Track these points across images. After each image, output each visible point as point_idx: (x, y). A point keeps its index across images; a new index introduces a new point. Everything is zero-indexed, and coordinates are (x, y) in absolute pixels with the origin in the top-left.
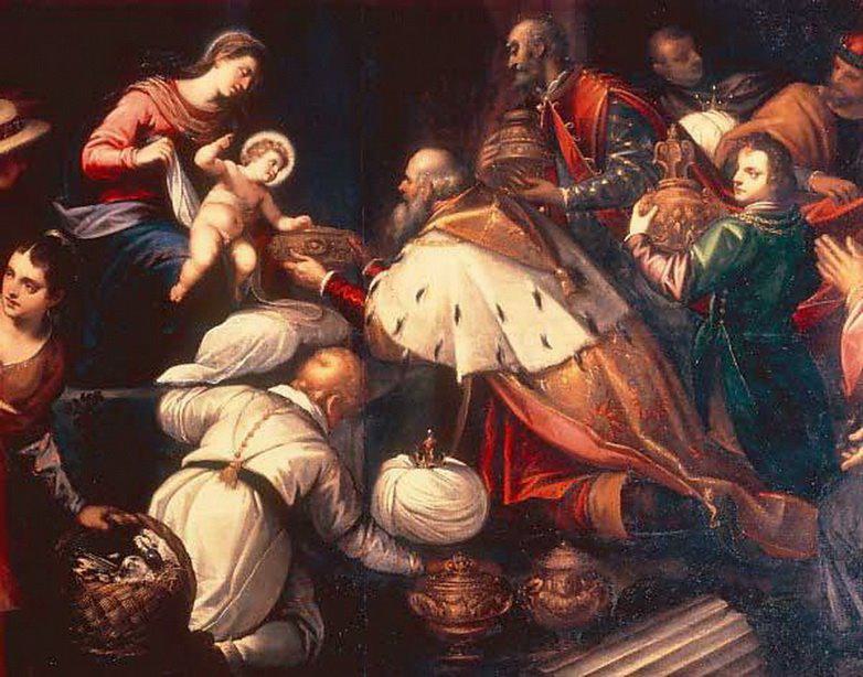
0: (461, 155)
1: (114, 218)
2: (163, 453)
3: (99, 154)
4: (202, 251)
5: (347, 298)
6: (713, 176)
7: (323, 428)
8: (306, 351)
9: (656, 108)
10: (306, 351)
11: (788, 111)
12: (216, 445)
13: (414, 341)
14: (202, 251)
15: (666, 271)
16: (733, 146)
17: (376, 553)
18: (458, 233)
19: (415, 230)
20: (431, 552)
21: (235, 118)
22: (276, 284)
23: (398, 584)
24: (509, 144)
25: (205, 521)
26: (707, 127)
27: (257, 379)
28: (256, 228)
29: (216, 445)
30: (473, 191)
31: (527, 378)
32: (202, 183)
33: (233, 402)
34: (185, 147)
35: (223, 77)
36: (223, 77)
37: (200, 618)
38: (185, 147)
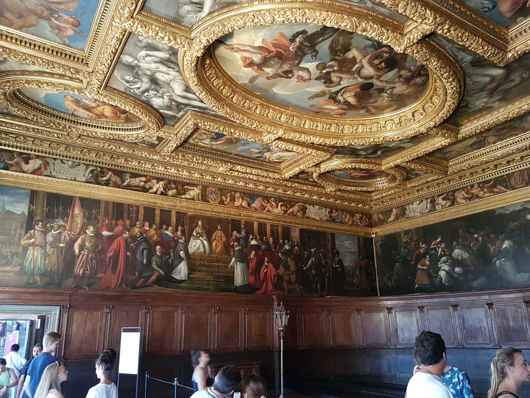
0: (457, 242)
1: (433, 252)
2: (439, 269)
3: (432, 247)
4: (439, 253)
5: (450, 255)
6: (477, 240)
7: (449, 265)
8: (448, 260)
9: (472, 234)
10: (448, 260)
11: (482, 233)
12: (443, 268)
13: (455, 258)
14: (439, 253)
15: (475, 248)
16: (478, 237)
17: (455, 275)
18: (458, 248)
19: (455, 249)
20: (459, 275)
21: (440, 242)
22: (445, 255)
23: (457, 277)
24: (461, 240)
25: (442, 274)
26: (476, 236)
27: (444, 263)
28: (443, 251)
29: (443, 268)
30: (458, 245)
31: (465, 259)
32: (439, 248)
33: (443, 264)
34: (437, 245)
35: (439, 239)
36: (439, 239)
37: (443, 282)
38: (437, 245)
